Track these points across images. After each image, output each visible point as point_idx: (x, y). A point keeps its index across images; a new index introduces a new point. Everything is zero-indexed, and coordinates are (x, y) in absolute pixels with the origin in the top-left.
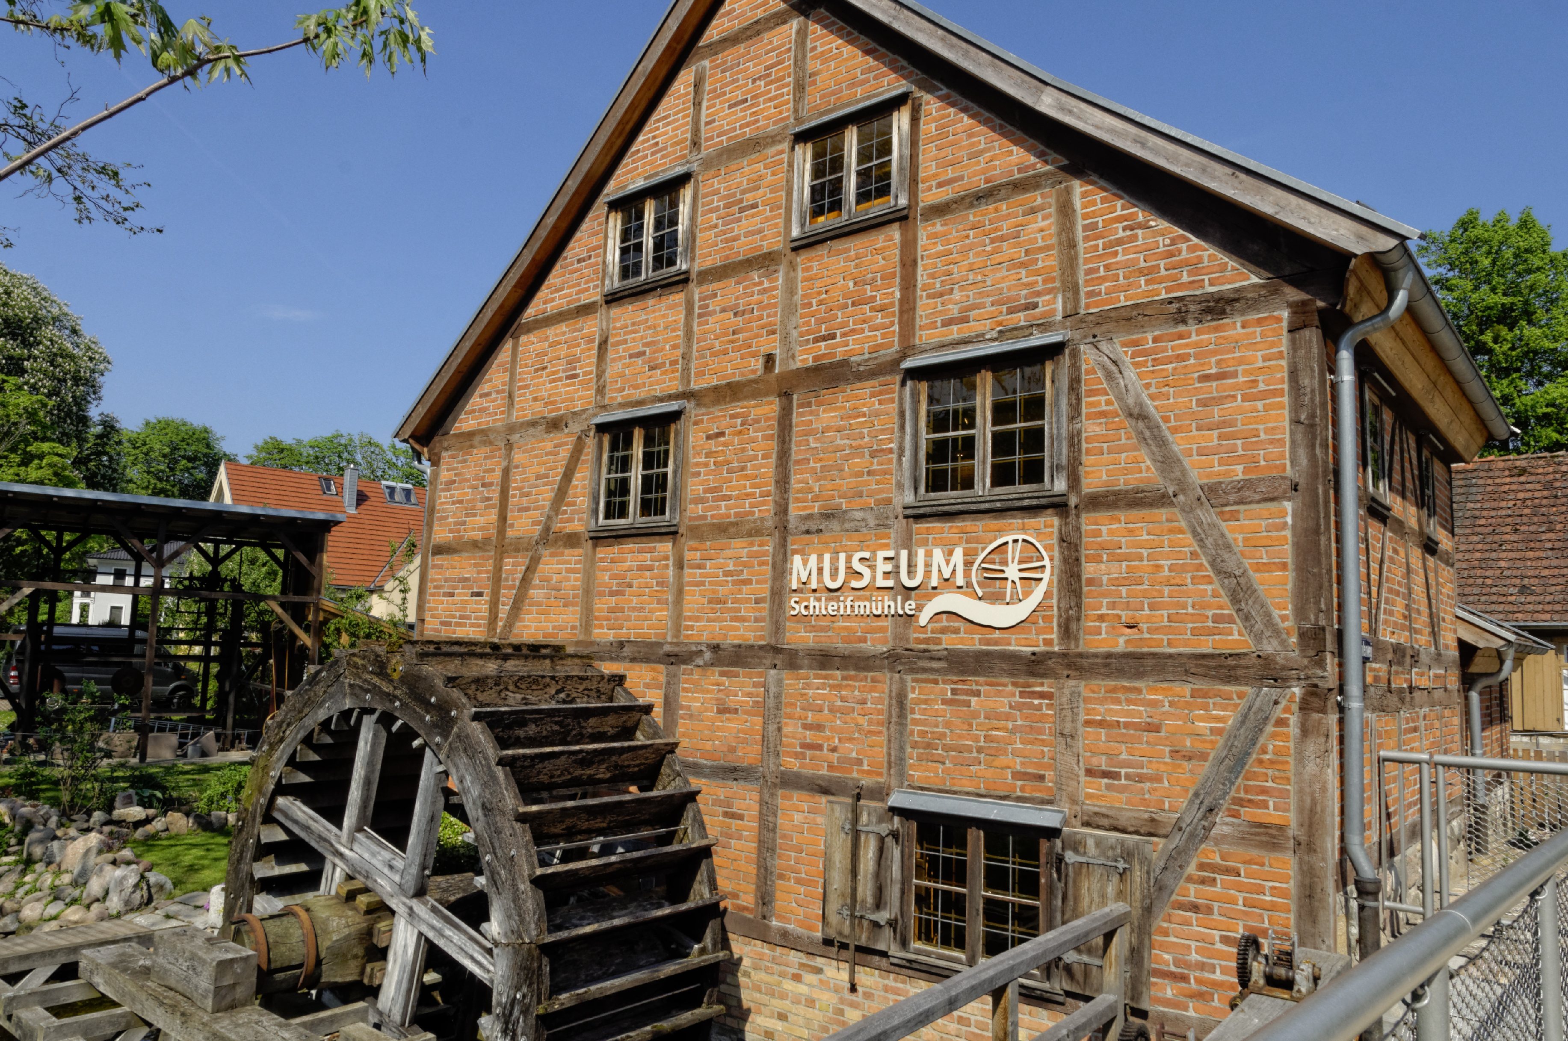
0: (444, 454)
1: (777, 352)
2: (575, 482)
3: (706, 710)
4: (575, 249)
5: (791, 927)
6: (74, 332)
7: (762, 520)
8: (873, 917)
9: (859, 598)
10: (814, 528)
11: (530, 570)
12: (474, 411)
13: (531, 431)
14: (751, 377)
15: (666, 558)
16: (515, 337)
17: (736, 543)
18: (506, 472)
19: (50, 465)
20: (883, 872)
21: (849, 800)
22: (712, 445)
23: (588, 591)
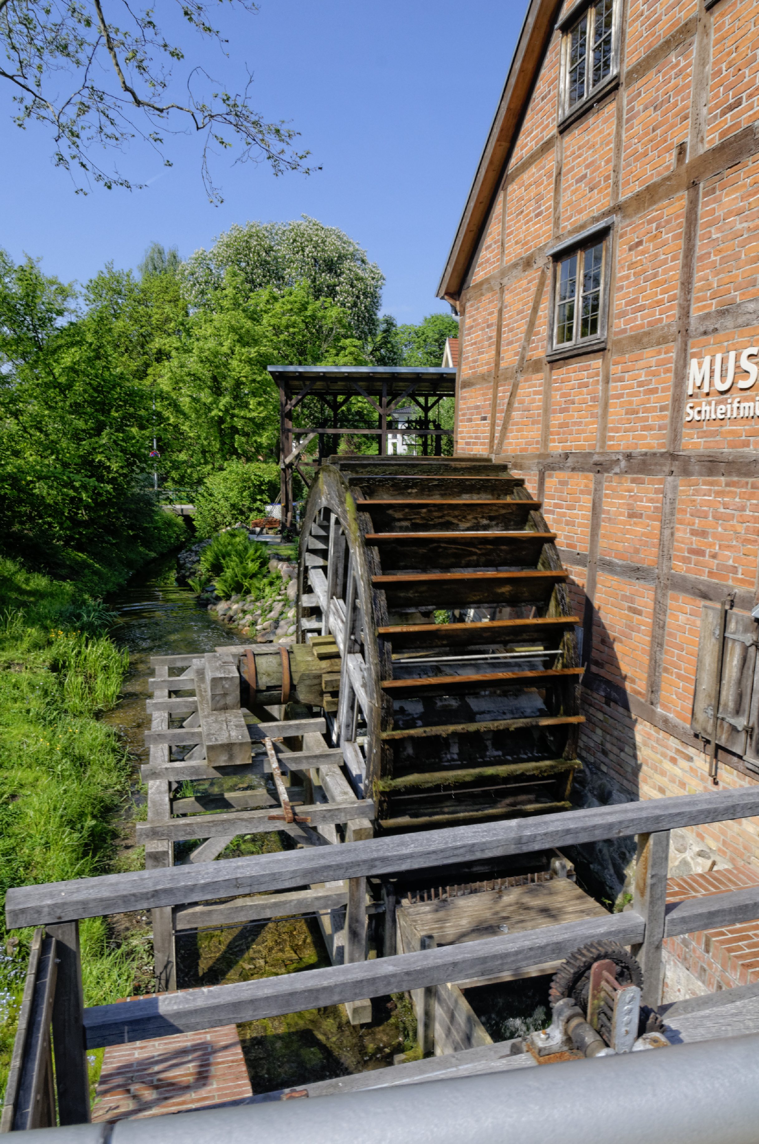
0: (468, 304)
1: (688, 140)
2: (540, 313)
3: (621, 514)
4: (541, 86)
5: (671, 716)
6: (363, 261)
7: (669, 325)
8: (732, 721)
9: (746, 399)
10: (712, 327)
11: (512, 395)
12: (482, 263)
13: (515, 272)
14: (666, 174)
15: (597, 375)
16: (505, 189)
17: (648, 352)
18: (500, 311)
19: (351, 353)
20: (744, 681)
21: (718, 606)
23: (546, 410)
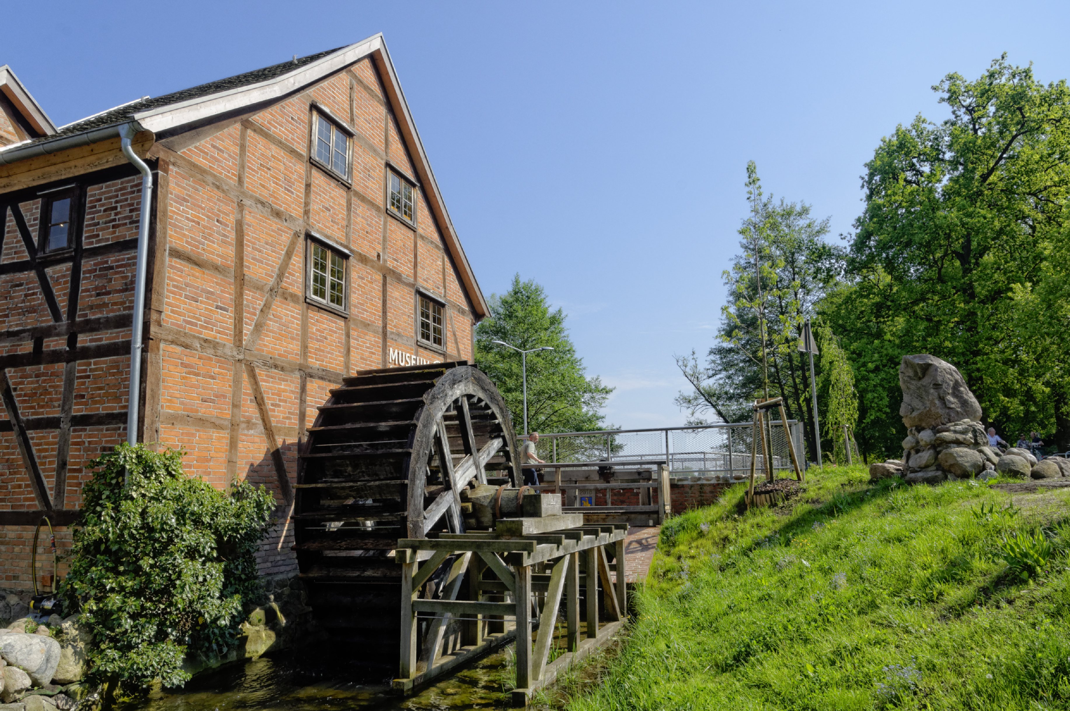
2: (292, 261)
17: (370, 333)
22: (360, 282)
